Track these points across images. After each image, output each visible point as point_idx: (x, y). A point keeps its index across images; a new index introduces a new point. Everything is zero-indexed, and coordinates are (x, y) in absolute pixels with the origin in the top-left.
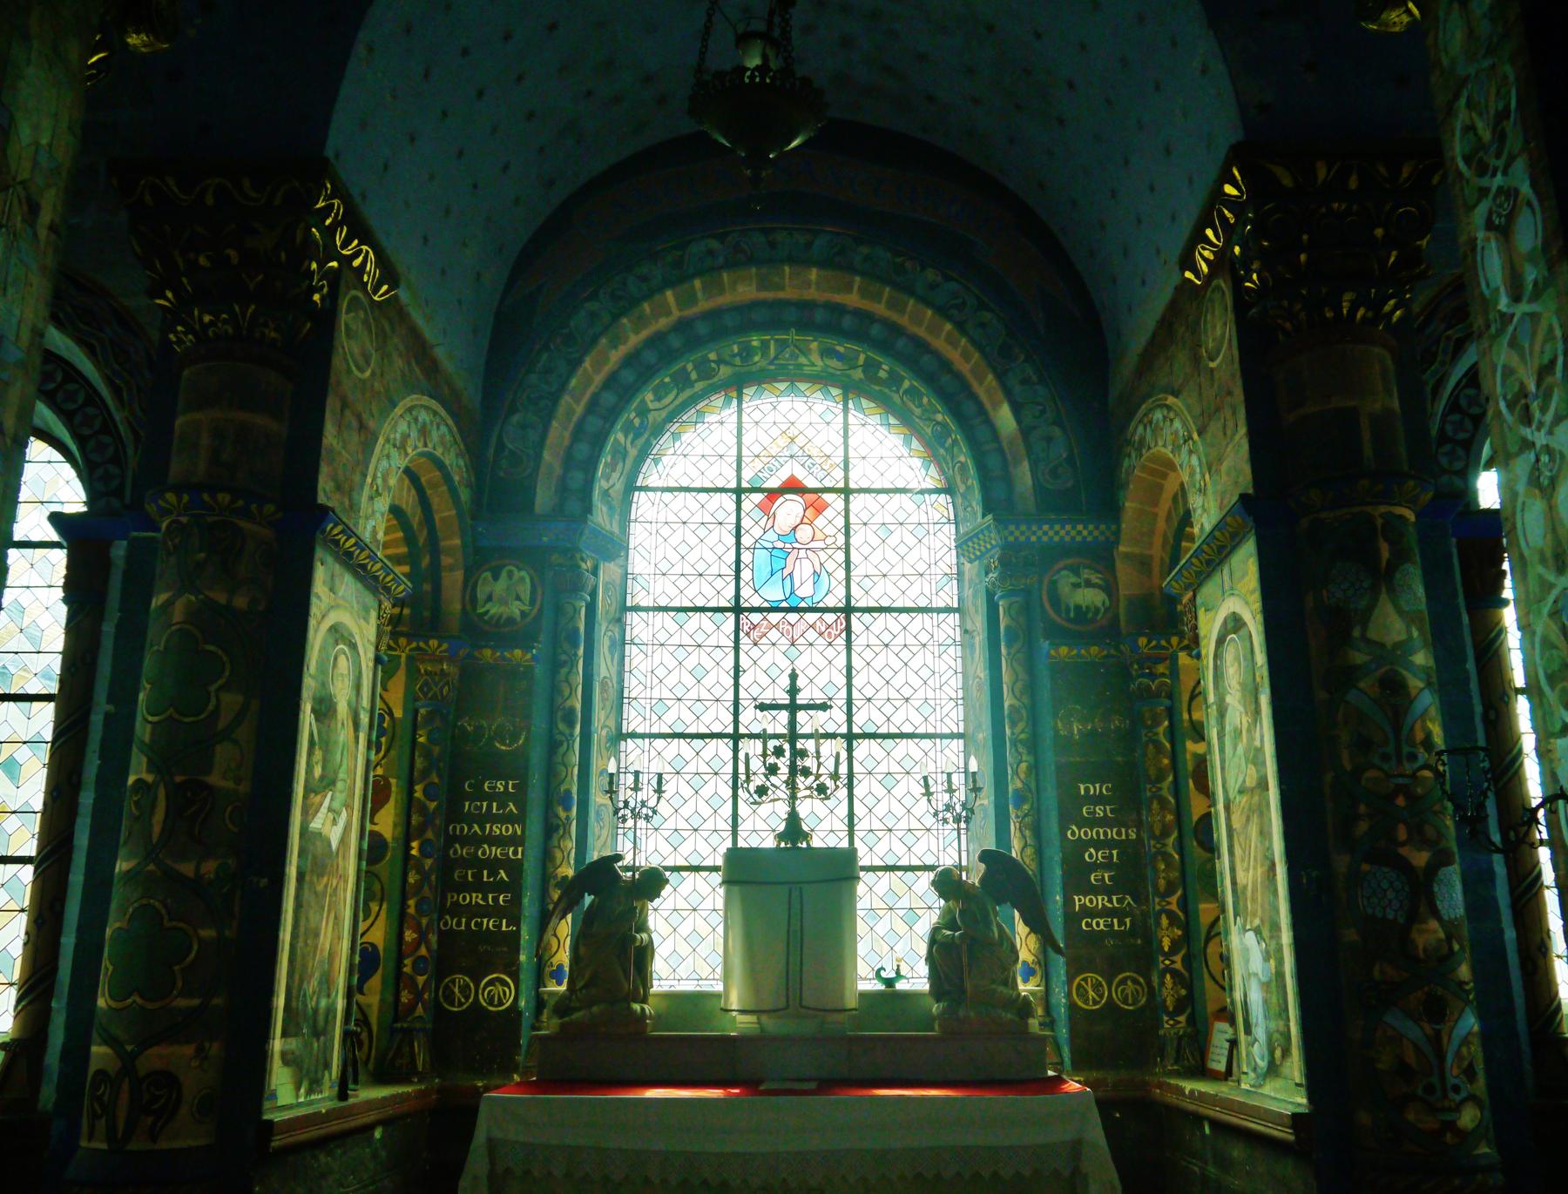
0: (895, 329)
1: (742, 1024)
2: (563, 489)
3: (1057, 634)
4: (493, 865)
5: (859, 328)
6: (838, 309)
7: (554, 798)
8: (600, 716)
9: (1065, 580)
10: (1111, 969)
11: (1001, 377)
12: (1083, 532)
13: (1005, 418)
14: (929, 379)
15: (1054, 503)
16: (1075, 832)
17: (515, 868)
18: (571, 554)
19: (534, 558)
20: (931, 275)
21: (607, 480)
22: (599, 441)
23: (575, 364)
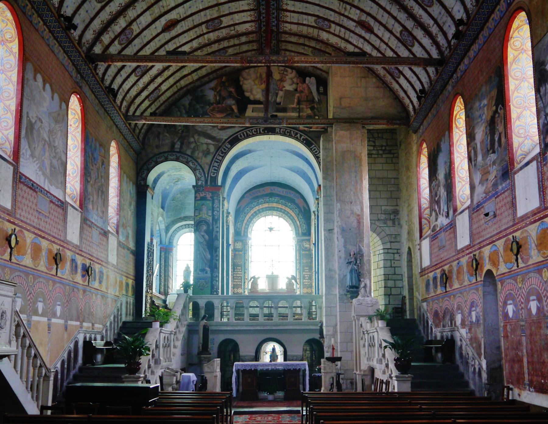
0: (285, 211)
1: (267, 291)
2: (244, 232)
3: (303, 250)
4: (239, 277)
5: (281, 210)
6: (278, 208)
7: (245, 269)
8: (250, 259)
9: (304, 243)
10: (307, 288)
11: (298, 218)
12: (307, 238)
13: (298, 222)
14: (289, 217)
15: (304, 234)
16: (304, 273)
17: (241, 277)
18: (246, 240)
19: (242, 241)
20: (290, 204)
21: (249, 230)
22: (248, 225)
23: (246, 216)
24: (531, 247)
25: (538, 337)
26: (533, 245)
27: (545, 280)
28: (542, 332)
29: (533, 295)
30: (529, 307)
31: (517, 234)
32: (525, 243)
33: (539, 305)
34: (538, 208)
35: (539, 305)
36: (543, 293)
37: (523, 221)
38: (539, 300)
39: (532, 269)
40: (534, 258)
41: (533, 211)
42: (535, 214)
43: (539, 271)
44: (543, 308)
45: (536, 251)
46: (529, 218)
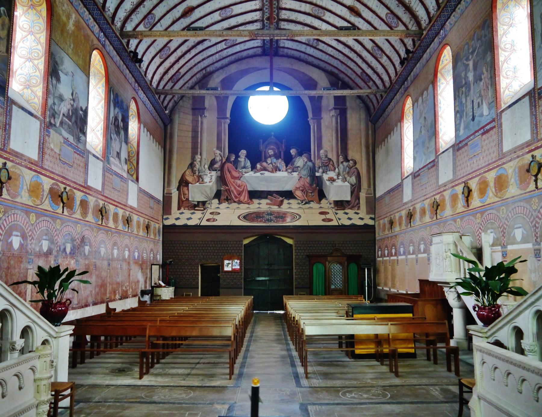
24: (22, 188)
25: (16, 270)
26: (25, 187)
27: (33, 223)
28: (22, 266)
29: (17, 231)
30: (10, 241)
31: (9, 164)
32: (15, 179)
33: (22, 242)
34: (35, 161)
35: (22, 242)
36: (28, 233)
37: (16, 156)
38: (24, 236)
39: (20, 208)
40: (24, 199)
41: (29, 158)
42: (32, 163)
43: (27, 213)
44: (27, 246)
45: (27, 194)
46: (25, 160)
